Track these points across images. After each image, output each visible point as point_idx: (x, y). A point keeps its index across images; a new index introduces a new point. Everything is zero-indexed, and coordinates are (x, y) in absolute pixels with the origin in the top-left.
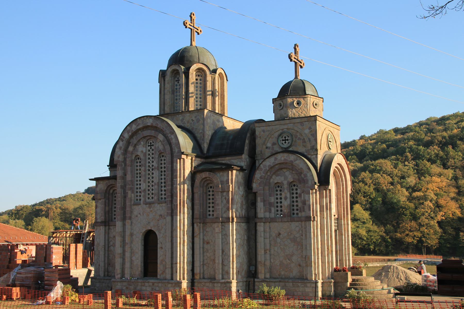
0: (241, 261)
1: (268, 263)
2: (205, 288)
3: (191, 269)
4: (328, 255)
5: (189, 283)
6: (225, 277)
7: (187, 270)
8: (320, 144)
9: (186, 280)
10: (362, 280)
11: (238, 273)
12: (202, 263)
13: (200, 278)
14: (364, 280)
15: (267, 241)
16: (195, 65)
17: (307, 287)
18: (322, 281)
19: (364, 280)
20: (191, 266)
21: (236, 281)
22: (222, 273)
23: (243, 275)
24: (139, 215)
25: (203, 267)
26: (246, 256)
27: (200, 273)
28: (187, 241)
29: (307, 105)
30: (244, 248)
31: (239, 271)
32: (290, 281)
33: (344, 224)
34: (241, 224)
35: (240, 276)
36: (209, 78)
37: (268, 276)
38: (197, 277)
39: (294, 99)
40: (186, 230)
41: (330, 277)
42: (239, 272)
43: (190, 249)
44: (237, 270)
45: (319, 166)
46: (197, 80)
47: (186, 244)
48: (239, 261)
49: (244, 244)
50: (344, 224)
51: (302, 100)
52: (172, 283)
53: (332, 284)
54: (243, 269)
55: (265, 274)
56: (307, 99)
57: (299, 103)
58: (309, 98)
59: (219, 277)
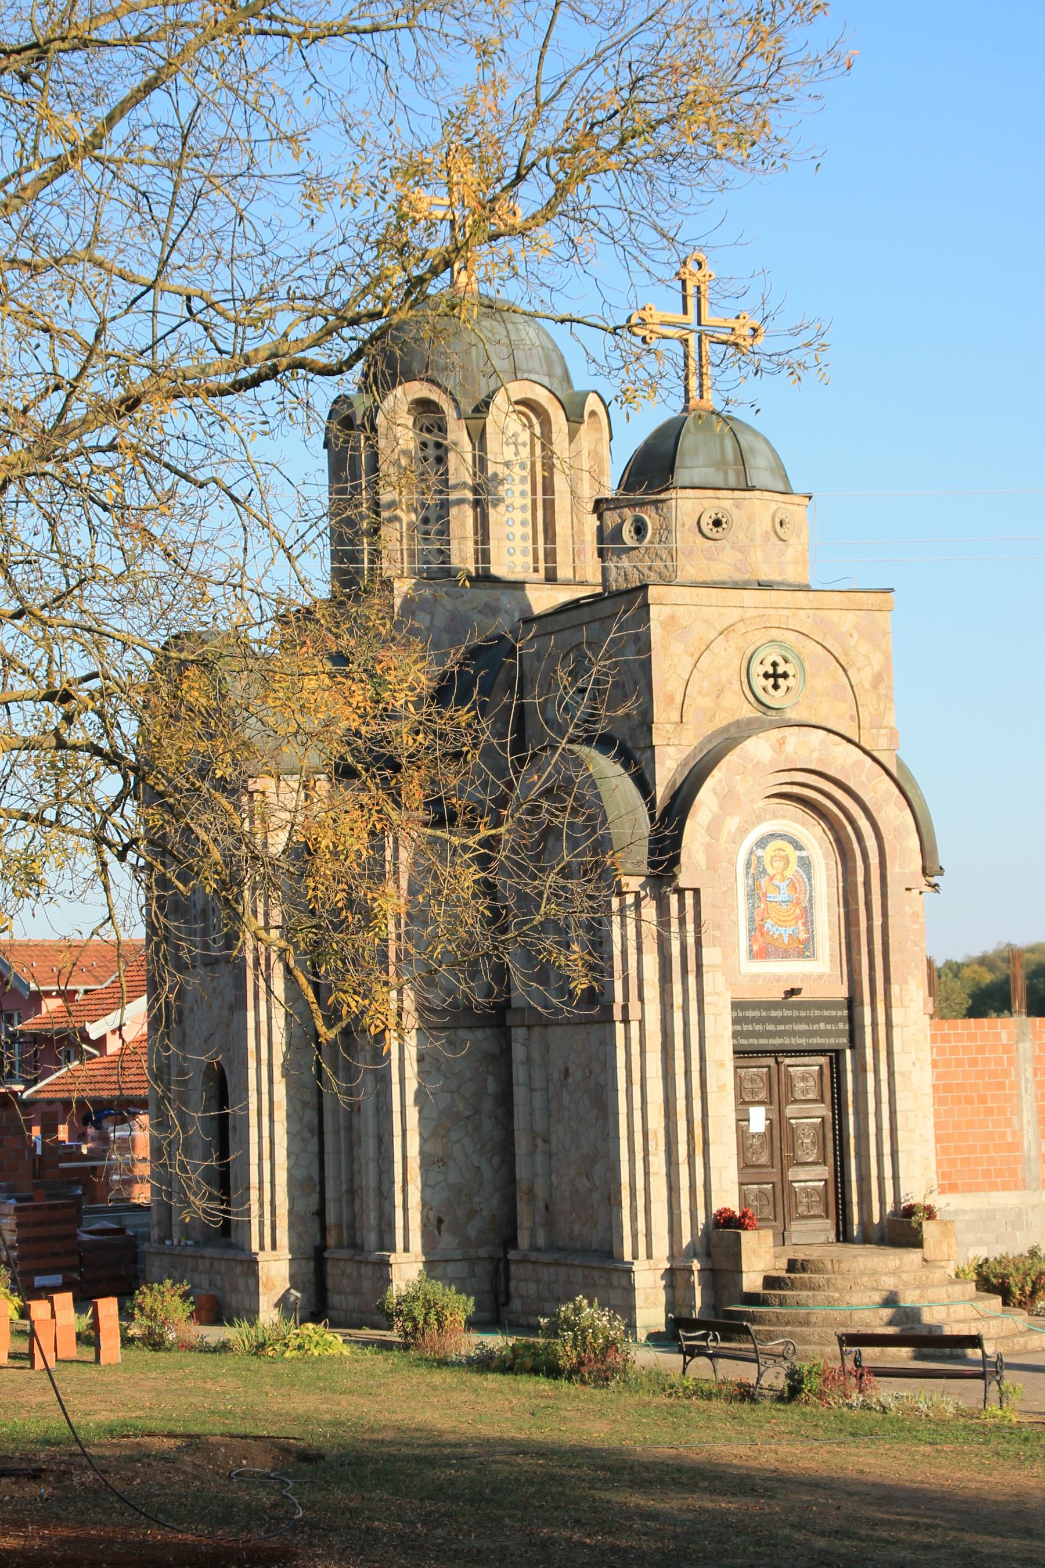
0: (453, 1178)
1: (540, 1189)
2: (345, 1281)
3: (315, 1207)
4: (691, 1156)
5: (303, 1262)
6: (387, 1242)
7: (291, 1211)
8: (679, 699)
9: (284, 1252)
10: (821, 1265)
11: (433, 1227)
12: (344, 1187)
13: (340, 1245)
14: (829, 1266)
15: (538, 1101)
16: (416, 385)
17: (612, 1287)
18: (668, 1266)
19: (829, 1266)
20: (315, 1197)
21: (424, 1259)
22: (379, 1225)
23: (472, 1231)
24: (195, 1008)
25: (352, 1201)
26: (496, 1160)
27: (339, 1226)
28: (284, 1102)
29: (670, 532)
30: (478, 1128)
31: (446, 1220)
32: (576, 1262)
33: (874, 1024)
34: (462, 1033)
35: (447, 1241)
36: (457, 434)
37: (541, 1242)
38: (331, 1240)
39: (626, 510)
40: (278, 1060)
41: (699, 1249)
42: (440, 1221)
43: (307, 1135)
44: (432, 1214)
45: (661, 792)
46: (424, 445)
47: (281, 1115)
48: (446, 1180)
49: (477, 1111)
50: (874, 1024)
51: (653, 514)
52: (242, 1262)
53: (696, 1278)
54: (472, 1213)
55: (533, 1235)
56: (669, 508)
57: (640, 529)
58: (673, 502)
59: (372, 1238)
